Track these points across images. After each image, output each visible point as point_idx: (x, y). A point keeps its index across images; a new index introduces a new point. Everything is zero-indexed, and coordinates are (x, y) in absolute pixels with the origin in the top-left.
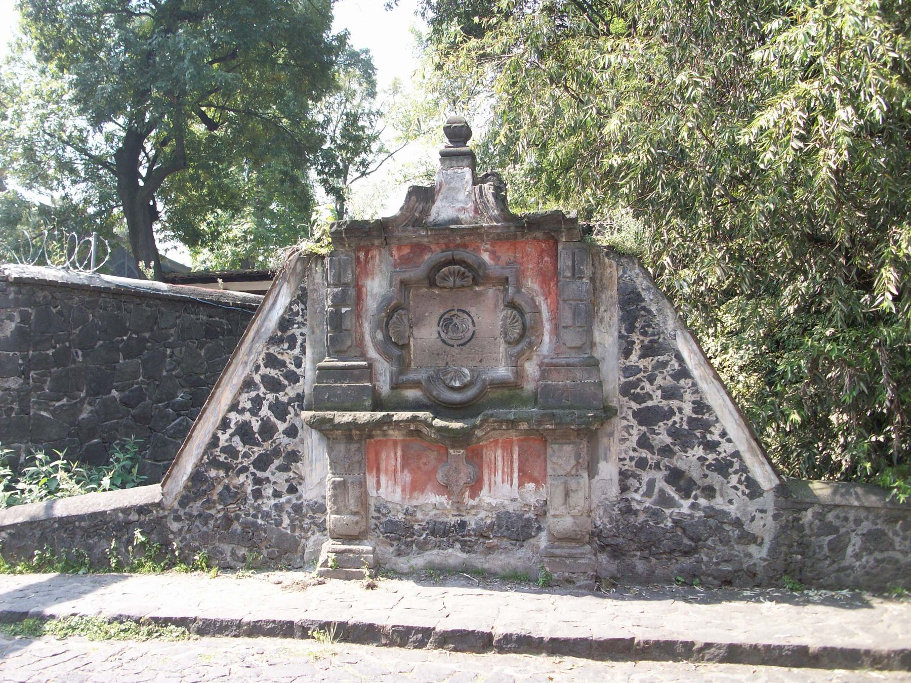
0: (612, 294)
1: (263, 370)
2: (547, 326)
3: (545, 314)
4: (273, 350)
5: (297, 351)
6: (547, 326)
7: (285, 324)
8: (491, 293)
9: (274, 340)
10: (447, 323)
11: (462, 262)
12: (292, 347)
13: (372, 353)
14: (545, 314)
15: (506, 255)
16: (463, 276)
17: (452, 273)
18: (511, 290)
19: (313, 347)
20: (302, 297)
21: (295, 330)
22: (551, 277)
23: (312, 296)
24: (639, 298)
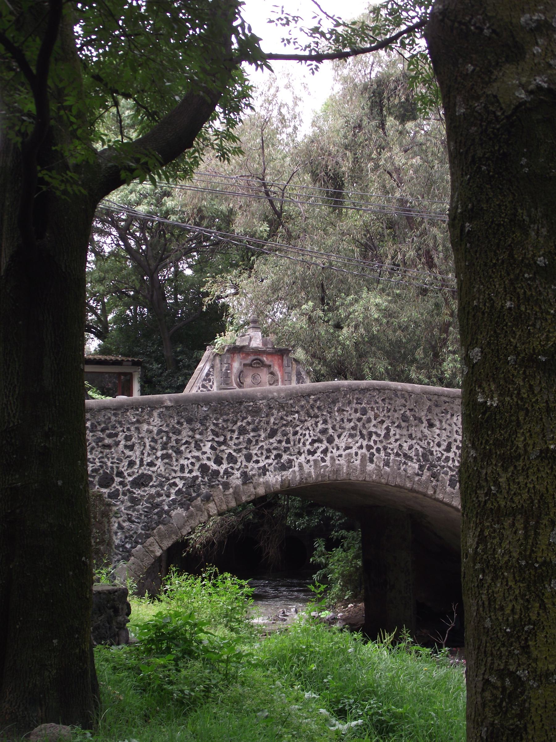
0: (294, 372)
1: (201, 389)
2: (280, 380)
3: (280, 377)
4: (204, 382)
5: (211, 383)
6: (280, 380)
7: (208, 375)
8: (265, 369)
9: (205, 380)
10: (254, 377)
11: (259, 360)
12: (210, 382)
13: (235, 385)
14: (280, 377)
15: (270, 359)
16: (259, 364)
17: (257, 363)
18: (272, 369)
19: (217, 382)
20: (212, 367)
21: (211, 377)
22: (281, 366)
23: (216, 367)
24: (301, 374)
